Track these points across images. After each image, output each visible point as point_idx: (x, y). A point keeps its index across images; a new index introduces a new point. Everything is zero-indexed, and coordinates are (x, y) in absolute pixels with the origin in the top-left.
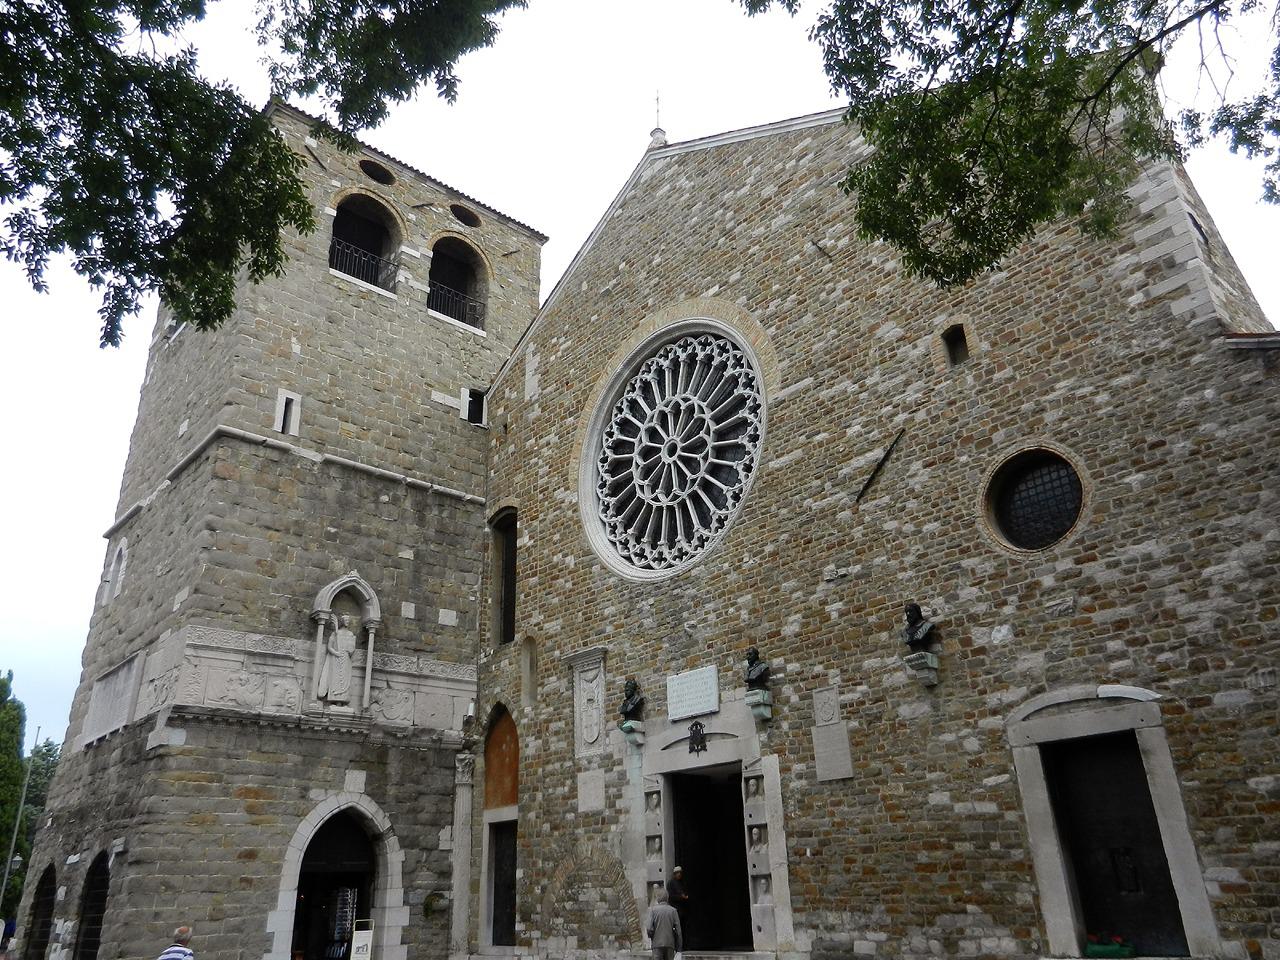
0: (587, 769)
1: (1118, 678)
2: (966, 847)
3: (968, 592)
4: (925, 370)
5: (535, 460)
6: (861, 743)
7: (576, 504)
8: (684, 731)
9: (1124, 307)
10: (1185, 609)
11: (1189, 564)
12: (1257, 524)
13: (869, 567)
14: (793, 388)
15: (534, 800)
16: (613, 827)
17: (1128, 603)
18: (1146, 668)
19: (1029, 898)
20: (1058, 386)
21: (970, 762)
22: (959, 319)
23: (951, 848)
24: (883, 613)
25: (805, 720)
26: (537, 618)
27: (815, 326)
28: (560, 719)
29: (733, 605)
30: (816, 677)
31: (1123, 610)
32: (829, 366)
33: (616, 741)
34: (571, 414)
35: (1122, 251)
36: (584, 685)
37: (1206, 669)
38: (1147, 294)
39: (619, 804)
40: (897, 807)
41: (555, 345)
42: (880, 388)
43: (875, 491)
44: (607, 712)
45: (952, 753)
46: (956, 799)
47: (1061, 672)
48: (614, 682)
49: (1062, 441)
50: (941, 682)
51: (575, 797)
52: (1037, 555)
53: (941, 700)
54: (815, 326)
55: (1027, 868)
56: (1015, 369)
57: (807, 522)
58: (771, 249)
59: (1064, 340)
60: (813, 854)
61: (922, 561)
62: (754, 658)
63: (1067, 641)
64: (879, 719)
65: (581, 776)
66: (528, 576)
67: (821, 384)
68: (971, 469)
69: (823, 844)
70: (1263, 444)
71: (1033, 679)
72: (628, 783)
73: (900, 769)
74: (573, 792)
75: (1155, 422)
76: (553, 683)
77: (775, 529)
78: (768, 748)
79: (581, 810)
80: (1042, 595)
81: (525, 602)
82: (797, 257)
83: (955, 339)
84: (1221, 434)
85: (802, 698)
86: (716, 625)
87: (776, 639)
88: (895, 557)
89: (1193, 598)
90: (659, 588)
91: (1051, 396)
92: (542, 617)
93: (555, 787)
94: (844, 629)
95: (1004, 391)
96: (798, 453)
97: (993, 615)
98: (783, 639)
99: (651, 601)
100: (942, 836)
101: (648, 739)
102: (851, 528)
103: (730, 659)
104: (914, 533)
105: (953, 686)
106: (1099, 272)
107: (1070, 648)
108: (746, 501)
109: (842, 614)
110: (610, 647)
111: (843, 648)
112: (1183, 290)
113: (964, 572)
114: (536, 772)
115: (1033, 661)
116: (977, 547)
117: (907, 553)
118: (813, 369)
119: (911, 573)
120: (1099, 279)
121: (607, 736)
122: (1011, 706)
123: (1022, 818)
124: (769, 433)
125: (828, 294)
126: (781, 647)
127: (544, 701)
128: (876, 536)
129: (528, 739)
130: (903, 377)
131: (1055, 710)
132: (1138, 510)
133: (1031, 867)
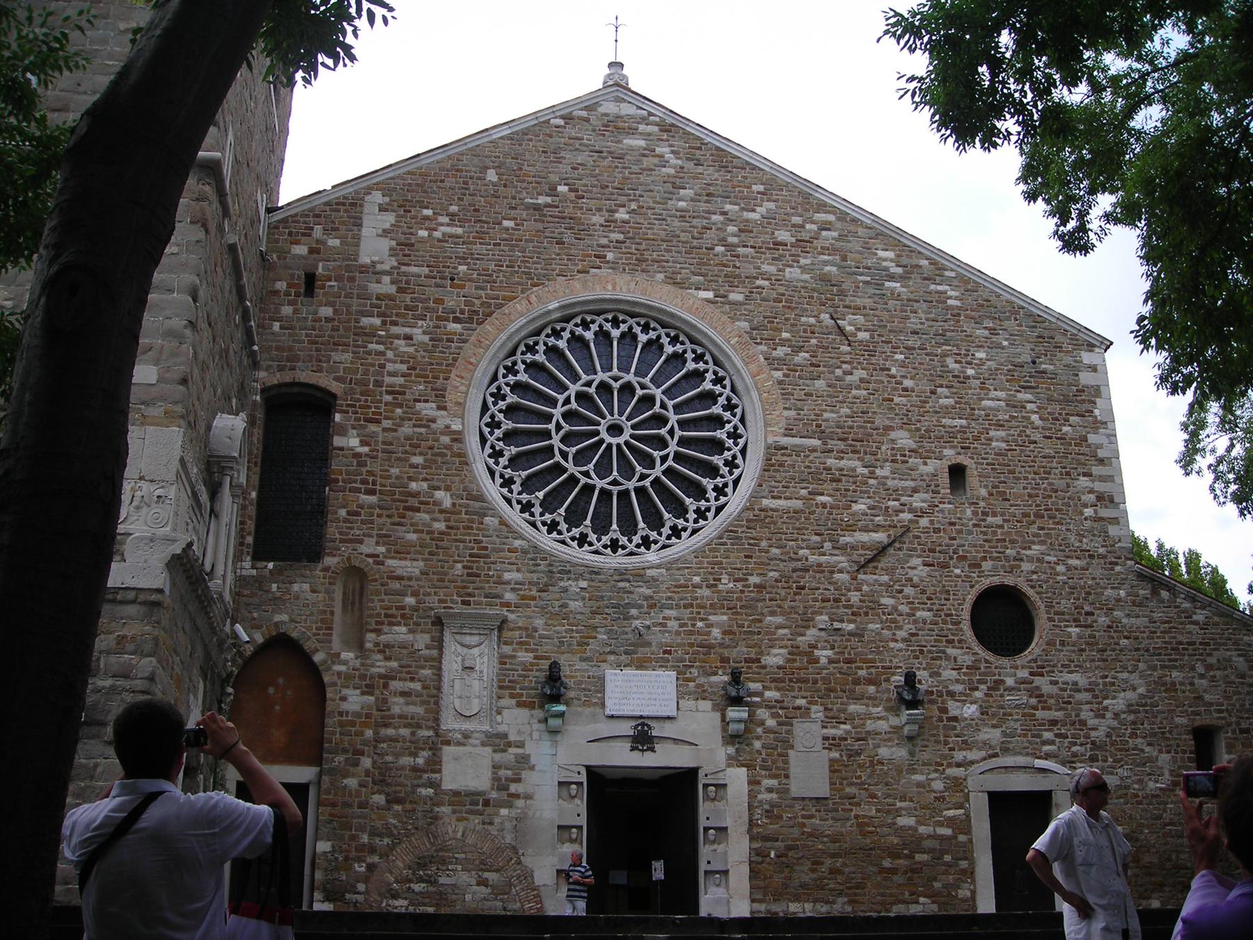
0: (459, 744)
1: (1047, 756)
2: (925, 857)
3: (949, 674)
4: (930, 485)
5: (381, 348)
6: (839, 771)
7: (459, 433)
8: (627, 728)
9: (1082, 513)
10: (1092, 722)
11: (1098, 694)
12: (1135, 682)
13: (864, 629)
14: (797, 441)
15: (357, 764)
16: (504, 811)
17: (1059, 710)
18: (1065, 754)
19: (968, 894)
20: (1033, 547)
21: (935, 797)
22: (963, 460)
23: (911, 857)
24: (873, 670)
25: (782, 744)
26: (368, 547)
27: (828, 396)
28: (412, 679)
29: (702, 620)
30: (799, 708)
31: (1056, 713)
32: (839, 440)
33: (515, 720)
34: (456, 320)
35: (1085, 475)
36: (459, 648)
37: (1098, 761)
38: (1096, 512)
39: (513, 788)
40: (868, 825)
41: (426, 218)
42: (890, 483)
43: (876, 568)
44: (500, 687)
45: (922, 790)
46: (919, 823)
47: (1011, 746)
48: (514, 657)
49: (1032, 587)
50: (919, 735)
51: (439, 771)
52: (1005, 661)
53: (917, 750)
54: (828, 396)
55: (970, 873)
56: (1005, 521)
57: (800, 570)
58: (783, 295)
59: (1039, 516)
60: (777, 856)
61: (913, 639)
62: (736, 678)
63: (1017, 725)
64: (859, 755)
65: (446, 749)
66: (358, 491)
67: (830, 451)
68: (963, 581)
69: (789, 848)
70: (1145, 635)
71: (990, 747)
72: (532, 768)
73: (873, 796)
74: (435, 764)
75: (1091, 598)
76: (400, 633)
77: (762, 563)
78: (733, 761)
79: (447, 785)
80: (1005, 690)
81: (345, 521)
82: (812, 320)
83: (957, 473)
84: (1125, 621)
85: (780, 724)
86: (678, 633)
87: (755, 665)
88: (889, 628)
89: (1097, 716)
90: (597, 573)
91: (1028, 552)
92: (382, 549)
93: (397, 756)
94: (833, 674)
95: (994, 533)
96: (798, 504)
97: (966, 695)
98: (764, 667)
99: (584, 584)
100: (905, 849)
101: (566, 727)
102: (849, 590)
103: (695, 672)
104: (909, 615)
105: (928, 740)
106: (1069, 481)
107: (1019, 731)
108: (731, 524)
109: (831, 661)
110: (511, 617)
111: (830, 690)
112: (1115, 521)
113: (948, 658)
114: (362, 734)
115: (992, 735)
116: (960, 641)
117: (900, 628)
118: (821, 434)
119: (900, 645)
120: (1068, 486)
121: (499, 713)
122: (972, 762)
123: (971, 841)
124: (765, 470)
125: (845, 373)
126: (759, 673)
127: (379, 651)
128: (871, 607)
129: (345, 692)
130: (912, 484)
131: (1003, 770)
132: (1074, 651)
133: (972, 873)
